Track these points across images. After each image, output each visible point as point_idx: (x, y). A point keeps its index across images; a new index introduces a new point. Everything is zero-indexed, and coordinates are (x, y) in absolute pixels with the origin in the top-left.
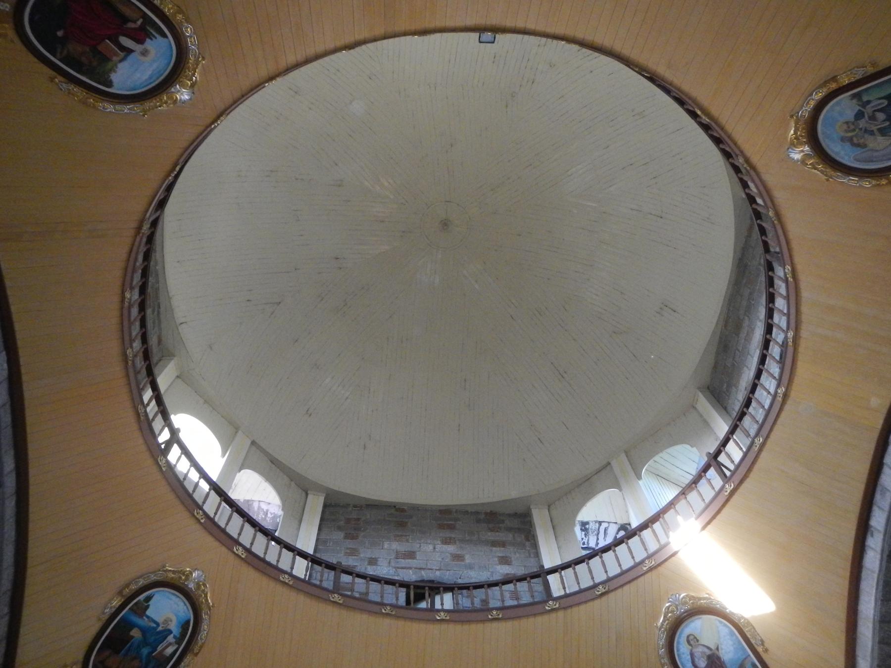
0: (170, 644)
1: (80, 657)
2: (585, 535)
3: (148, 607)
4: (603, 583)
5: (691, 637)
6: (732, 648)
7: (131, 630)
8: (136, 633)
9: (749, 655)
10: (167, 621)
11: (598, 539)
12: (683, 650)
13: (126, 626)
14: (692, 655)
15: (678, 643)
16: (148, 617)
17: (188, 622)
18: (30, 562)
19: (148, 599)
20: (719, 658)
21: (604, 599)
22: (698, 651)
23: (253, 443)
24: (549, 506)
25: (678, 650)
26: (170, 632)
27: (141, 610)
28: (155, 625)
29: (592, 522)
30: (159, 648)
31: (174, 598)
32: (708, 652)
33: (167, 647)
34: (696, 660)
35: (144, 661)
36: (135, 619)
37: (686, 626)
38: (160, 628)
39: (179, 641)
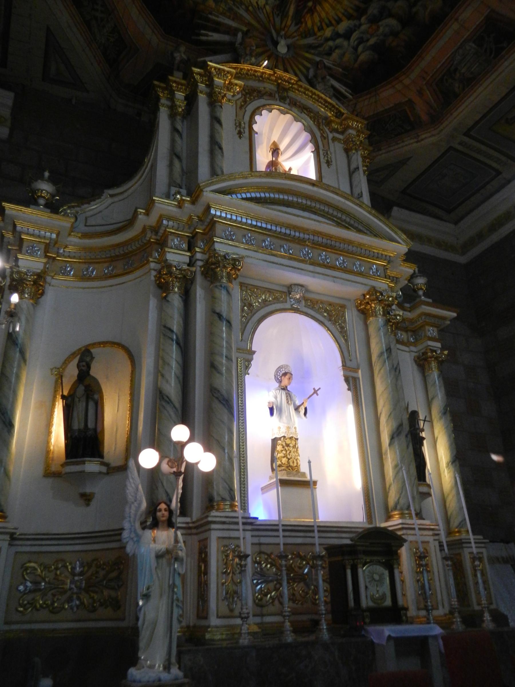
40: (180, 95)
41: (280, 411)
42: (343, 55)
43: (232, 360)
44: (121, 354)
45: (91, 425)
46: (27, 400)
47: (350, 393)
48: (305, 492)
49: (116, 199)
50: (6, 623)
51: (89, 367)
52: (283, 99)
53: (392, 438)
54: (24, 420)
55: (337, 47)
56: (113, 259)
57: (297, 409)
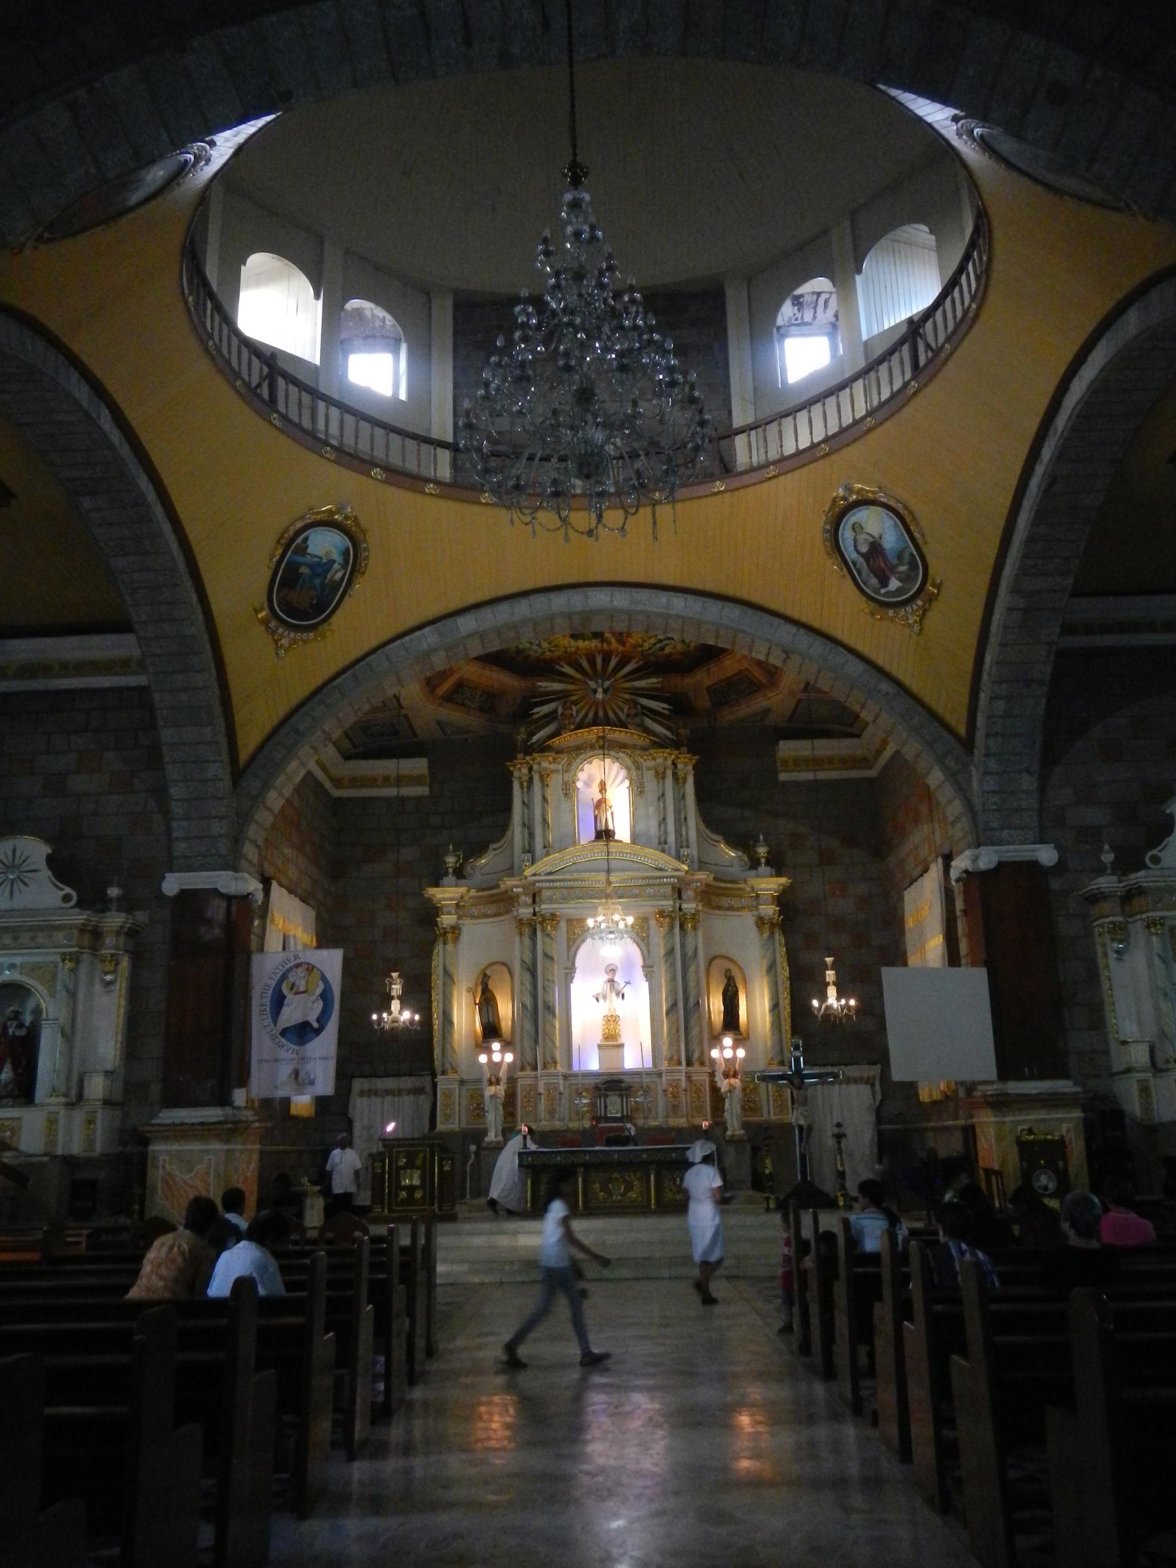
0: (337, 571)
1: (264, 598)
2: (799, 310)
3: (307, 546)
4: (775, 463)
5: (857, 525)
6: (893, 538)
7: (299, 568)
8: (304, 570)
9: (909, 546)
10: (327, 554)
11: (815, 312)
12: (847, 535)
13: (292, 568)
14: (855, 540)
15: (844, 529)
16: (310, 555)
17: (347, 549)
18: (193, 543)
19: (306, 540)
20: (880, 545)
21: (774, 481)
22: (862, 538)
23: (347, 252)
24: (749, 281)
25: (843, 535)
26: (334, 561)
27: (303, 550)
28: (317, 560)
29: (808, 293)
30: (329, 576)
31: (328, 533)
32: (871, 540)
33: (336, 573)
34: (859, 545)
35: (319, 588)
36: (300, 559)
37: (854, 514)
38: (324, 561)
39: (344, 566)
40: (525, 771)
41: (605, 997)
42: (675, 647)
43: (553, 982)
44: (505, 969)
45: (491, 1020)
46: (460, 1005)
47: (647, 984)
48: (615, 1052)
49: (497, 852)
50: (467, 1123)
51: (487, 985)
52: (602, 747)
53: (667, 1014)
54: (460, 1017)
55: (666, 645)
56: (498, 902)
57: (617, 994)
